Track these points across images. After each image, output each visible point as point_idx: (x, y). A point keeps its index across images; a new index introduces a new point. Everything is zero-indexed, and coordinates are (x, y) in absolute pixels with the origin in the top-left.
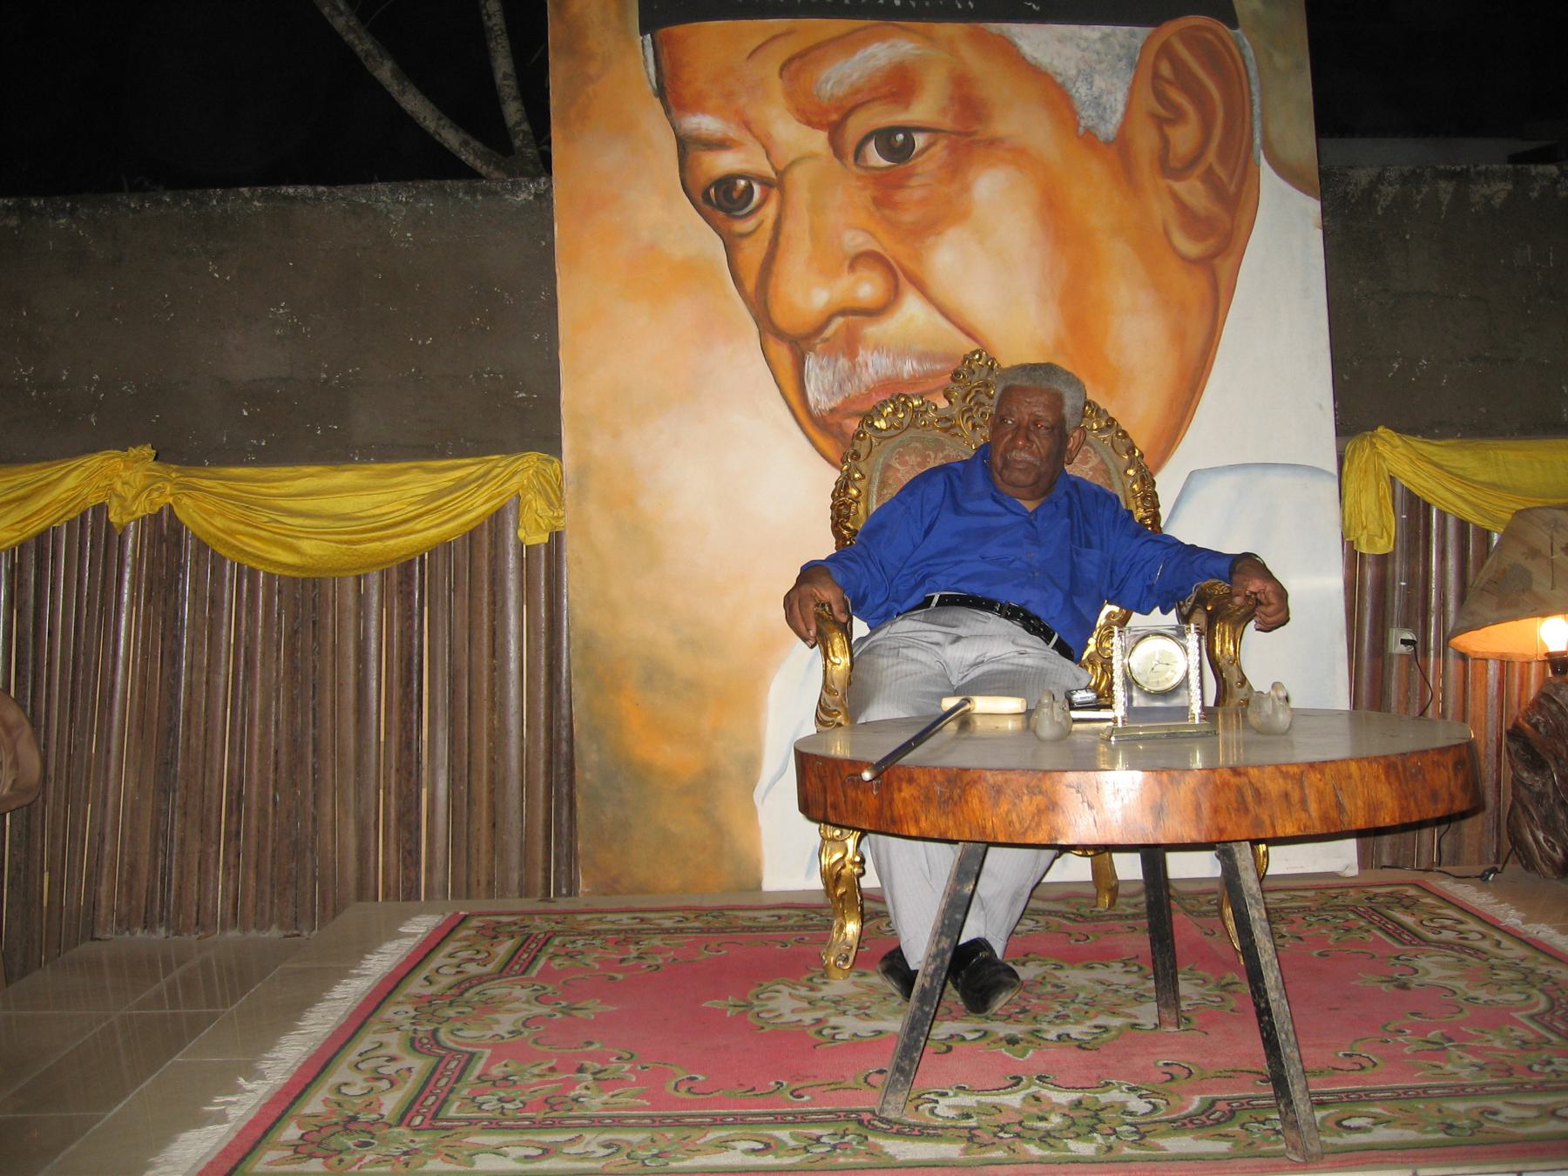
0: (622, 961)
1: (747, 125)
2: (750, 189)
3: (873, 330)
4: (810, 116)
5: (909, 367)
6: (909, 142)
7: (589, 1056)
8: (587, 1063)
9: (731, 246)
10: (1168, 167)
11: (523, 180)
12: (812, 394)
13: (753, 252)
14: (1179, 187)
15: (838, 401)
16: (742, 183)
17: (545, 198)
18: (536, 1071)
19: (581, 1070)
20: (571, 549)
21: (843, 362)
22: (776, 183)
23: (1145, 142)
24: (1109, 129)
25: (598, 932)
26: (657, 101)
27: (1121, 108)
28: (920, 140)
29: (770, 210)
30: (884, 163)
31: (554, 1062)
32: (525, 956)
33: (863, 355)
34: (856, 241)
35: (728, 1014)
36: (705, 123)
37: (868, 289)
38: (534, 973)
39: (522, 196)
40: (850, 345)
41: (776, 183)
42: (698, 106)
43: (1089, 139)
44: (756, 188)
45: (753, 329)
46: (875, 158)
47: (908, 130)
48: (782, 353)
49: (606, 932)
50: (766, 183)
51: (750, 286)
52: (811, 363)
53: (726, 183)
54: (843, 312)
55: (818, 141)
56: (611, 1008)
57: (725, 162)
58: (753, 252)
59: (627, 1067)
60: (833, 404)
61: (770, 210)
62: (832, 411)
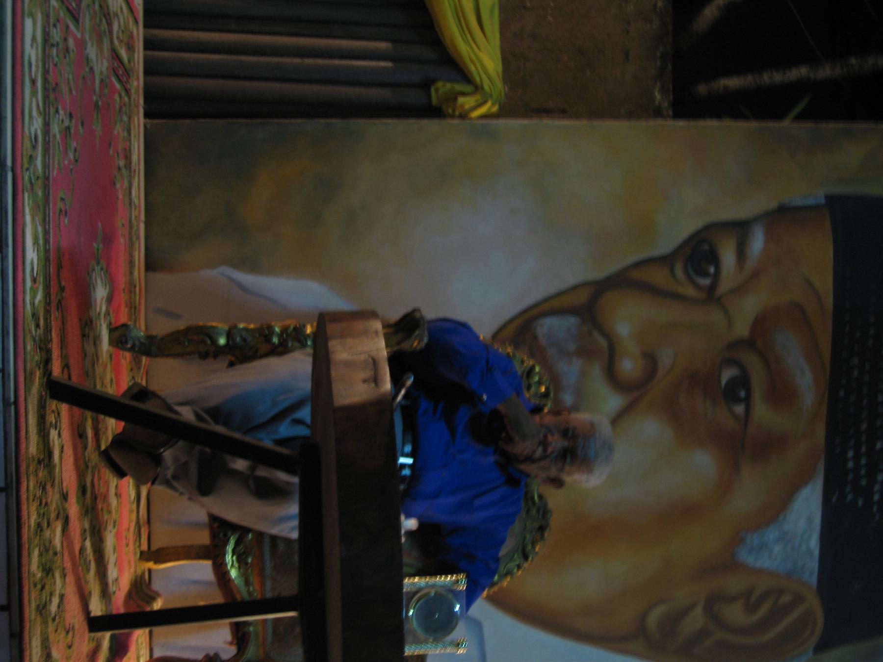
0: (118, 153)
1: (756, 275)
2: (705, 274)
3: (597, 370)
4: (761, 324)
6: (738, 400)
7: (76, 125)
8: (74, 121)
9: (666, 260)
10: (713, 602)
11: (671, 97)
13: (659, 277)
15: (543, 341)
16: (712, 270)
17: (657, 113)
18: (71, 77)
19: (71, 116)
20: (430, 126)
21: (572, 346)
22: (711, 296)
23: (733, 584)
24: (745, 556)
25: (130, 135)
26: (773, 205)
27: (759, 564)
28: (740, 409)
29: (690, 291)
30: (724, 381)
31: (74, 93)
32: (121, 72)
33: (577, 364)
34: (666, 358)
35: (95, 245)
36: (757, 243)
37: (629, 366)
38: (113, 79)
39: (658, 96)
40: (586, 352)
41: (711, 296)
42: (771, 237)
43: (737, 540)
44: (706, 282)
46: (727, 375)
47: (748, 401)
48: (581, 298)
49: (130, 140)
50: (712, 288)
51: (636, 274)
52: (572, 321)
53: (714, 258)
55: (742, 329)
56: (97, 142)
57: (728, 257)
58: (659, 277)
59: (72, 156)
60: (540, 337)
61: (690, 291)
62: (535, 338)
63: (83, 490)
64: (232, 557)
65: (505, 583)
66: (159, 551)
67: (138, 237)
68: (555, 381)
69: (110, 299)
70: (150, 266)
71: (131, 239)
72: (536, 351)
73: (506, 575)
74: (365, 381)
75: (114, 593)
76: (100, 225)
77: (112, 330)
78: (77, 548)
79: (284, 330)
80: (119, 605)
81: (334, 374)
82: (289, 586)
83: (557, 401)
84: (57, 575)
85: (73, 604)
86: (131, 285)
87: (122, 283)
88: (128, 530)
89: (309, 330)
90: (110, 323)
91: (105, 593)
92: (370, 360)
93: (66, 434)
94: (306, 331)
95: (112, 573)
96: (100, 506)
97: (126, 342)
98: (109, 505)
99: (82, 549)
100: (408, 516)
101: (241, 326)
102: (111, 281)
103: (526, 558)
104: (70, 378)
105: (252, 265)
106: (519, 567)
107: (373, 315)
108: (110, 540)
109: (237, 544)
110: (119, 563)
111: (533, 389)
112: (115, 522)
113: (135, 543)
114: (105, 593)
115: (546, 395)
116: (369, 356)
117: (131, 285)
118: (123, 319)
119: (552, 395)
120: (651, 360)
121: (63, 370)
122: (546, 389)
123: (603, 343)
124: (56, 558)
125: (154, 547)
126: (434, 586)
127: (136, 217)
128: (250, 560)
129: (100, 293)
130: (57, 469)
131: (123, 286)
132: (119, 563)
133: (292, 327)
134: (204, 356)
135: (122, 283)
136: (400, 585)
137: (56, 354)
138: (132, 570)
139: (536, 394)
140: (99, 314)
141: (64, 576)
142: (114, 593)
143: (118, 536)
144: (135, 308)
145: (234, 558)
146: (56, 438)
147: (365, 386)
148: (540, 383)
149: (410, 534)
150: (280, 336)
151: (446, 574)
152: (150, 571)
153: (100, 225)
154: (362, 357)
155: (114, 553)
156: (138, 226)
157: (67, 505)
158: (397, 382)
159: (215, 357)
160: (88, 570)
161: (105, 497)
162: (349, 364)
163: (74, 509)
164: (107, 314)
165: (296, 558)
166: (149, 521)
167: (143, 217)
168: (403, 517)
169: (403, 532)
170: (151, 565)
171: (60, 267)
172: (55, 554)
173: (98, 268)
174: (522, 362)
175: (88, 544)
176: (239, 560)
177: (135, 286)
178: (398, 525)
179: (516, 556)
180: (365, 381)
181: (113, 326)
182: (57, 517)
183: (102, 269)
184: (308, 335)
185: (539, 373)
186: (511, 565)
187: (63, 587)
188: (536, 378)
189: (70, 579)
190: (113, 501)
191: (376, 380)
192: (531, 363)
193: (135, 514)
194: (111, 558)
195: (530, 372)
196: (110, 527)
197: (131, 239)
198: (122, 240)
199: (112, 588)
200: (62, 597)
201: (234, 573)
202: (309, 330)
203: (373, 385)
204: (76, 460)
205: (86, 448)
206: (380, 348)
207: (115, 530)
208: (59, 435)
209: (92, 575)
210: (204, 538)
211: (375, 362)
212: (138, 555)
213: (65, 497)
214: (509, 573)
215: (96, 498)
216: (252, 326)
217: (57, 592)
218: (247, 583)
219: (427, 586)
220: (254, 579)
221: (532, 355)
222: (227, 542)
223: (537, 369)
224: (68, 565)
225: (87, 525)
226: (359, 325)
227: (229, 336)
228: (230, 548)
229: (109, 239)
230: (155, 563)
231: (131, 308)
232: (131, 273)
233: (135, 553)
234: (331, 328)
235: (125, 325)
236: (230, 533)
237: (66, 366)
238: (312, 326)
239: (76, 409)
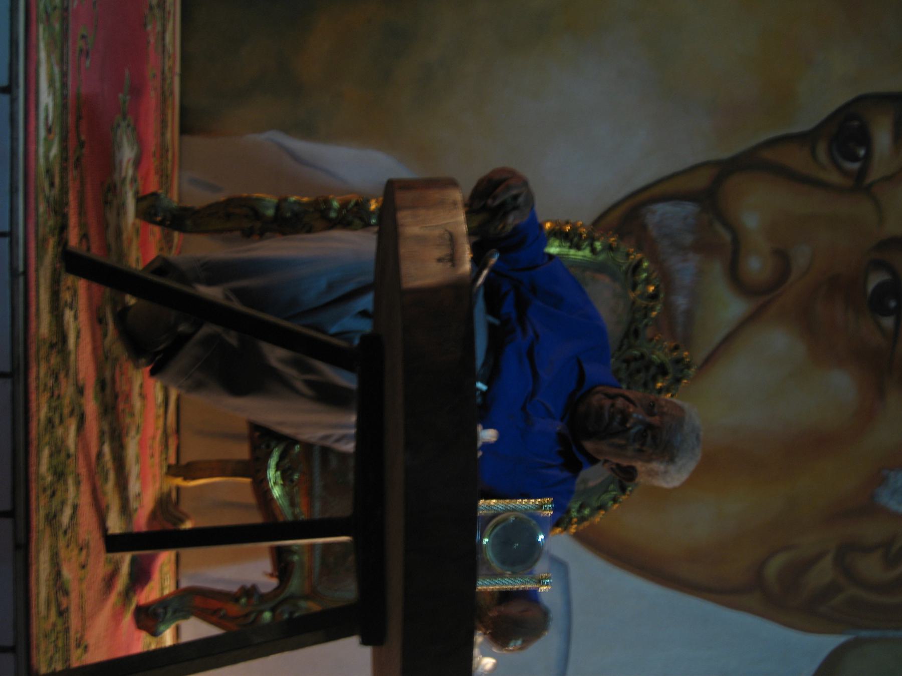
3: (717, 269)
5: (681, 302)
9: (807, 139)
12: (662, 209)
13: (797, 159)
14: (827, 562)
15: (654, 232)
21: (688, 239)
29: (834, 177)
34: (801, 258)
35: (121, 96)
45: (724, 154)
48: (701, 181)
52: (689, 208)
54: (736, 242)
58: (797, 159)
61: (834, 177)
62: (644, 227)
63: (102, 385)
64: (277, 471)
65: (598, 518)
66: (189, 465)
67: (172, 93)
68: (666, 281)
69: (137, 163)
70: (185, 130)
71: (163, 93)
72: (644, 242)
73: (600, 508)
74: (440, 260)
75: (136, 510)
76: (127, 73)
77: (139, 200)
78: (94, 451)
79: (344, 205)
80: (141, 522)
81: (403, 251)
82: (342, 507)
83: (668, 307)
84: (71, 481)
85: (87, 516)
86: (163, 151)
87: (152, 144)
88: (154, 438)
89: (373, 206)
90: (136, 193)
91: (125, 509)
92: (447, 236)
93: (83, 316)
94: (370, 206)
95: (134, 487)
96: (121, 406)
97: (156, 215)
98: (132, 407)
99: (100, 455)
100: (486, 427)
101: (293, 199)
102: (140, 141)
103: (623, 490)
104: (89, 249)
105: (307, 131)
106: (615, 500)
107: (451, 183)
108: (132, 449)
109: (282, 457)
110: (142, 476)
111: (640, 288)
112: (138, 427)
113: (162, 452)
114: (125, 509)
115: (654, 297)
116: (446, 230)
117: (163, 151)
118: (153, 187)
119: (662, 296)
120: (783, 258)
121: (81, 240)
122: (657, 288)
123: (727, 237)
124: (70, 460)
125: (184, 461)
126: (513, 510)
127: (170, 68)
128: (296, 477)
129: (127, 154)
130: (72, 357)
131: (153, 149)
132: (142, 476)
133: (352, 203)
134: (248, 234)
135: (152, 144)
136: (475, 507)
137: (73, 220)
138: (157, 485)
139: (641, 296)
140: (123, 181)
141: (78, 483)
142: (136, 510)
143: (141, 444)
144: (167, 177)
145: (279, 473)
146: (72, 319)
147: (440, 266)
148: (648, 282)
149: (487, 446)
150: (339, 211)
151: (529, 497)
152: (178, 489)
153: (127, 73)
154: (437, 232)
155: (137, 461)
156: (172, 78)
157: (83, 401)
158: (478, 261)
159: (262, 235)
160: (106, 480)
161: (128, 397)
162: (421, 240)
163: (91, 406)
164: (134, 180)
165: (351, 476)
166: (178, 431)
167: (178, 69)
168: (480, 428)
169: (480, 444)
170: (179, 481)
171: (79, 118)
172: (68, 456)
173: (124, 124)
174: (628, 255)
175: (106, 449)
176: (283, 477)
177: (167, 151)
178: (475, 436)
179: (612, 487)
180: (440, 260)
181: (140, 195)
182: (72, 413)
183: (129, 125)
184: (373, 212)
185: (646, 270)
186: (606, 497)
187: (75, 497)
188: (644, 275)
189: (85, 488)
190: (137, 403)
191: (453, 259)
192: (639, 256)
193: (161, 423)
194: (133, 470)
195: (637, 267)
196: (133, 433)
197: (163, 93)
198: (152, 94)
199: (134, 504)
200: (75, 508)
201: (276, 492)
202: (373, 206)
203: (449, 264)
204: (95, 349)
205: (105, 335)
206: (459, 222)
207: (138, 437)
208: (76, 317)
209: (110, 486)
210: (242, 452)
211: (452, 240)
212: (165, 470)
213: (80, 391)
214: (602, 507)
215: (116, 396)
216: (305, 199)
217: (70, 502)
218: (292, 504)
219: (506, 510)
220: (300, 499)
221: (639, 249)
222: (269, 455)
223: (646, 264)
224: (83, 471)
225: (106, 428)
226: (435, 195)
227: (278, 208)
228: (273, 462)
229: (137, 91)
230: (186, 478)
231: (161, 176)
232: (163, 134)
233: (161, 467)
234: (402, 197)
235: (155, 195)
236: (273, 444)
237: (85, 237)
238: (377, 202)
239: (95, 286)
